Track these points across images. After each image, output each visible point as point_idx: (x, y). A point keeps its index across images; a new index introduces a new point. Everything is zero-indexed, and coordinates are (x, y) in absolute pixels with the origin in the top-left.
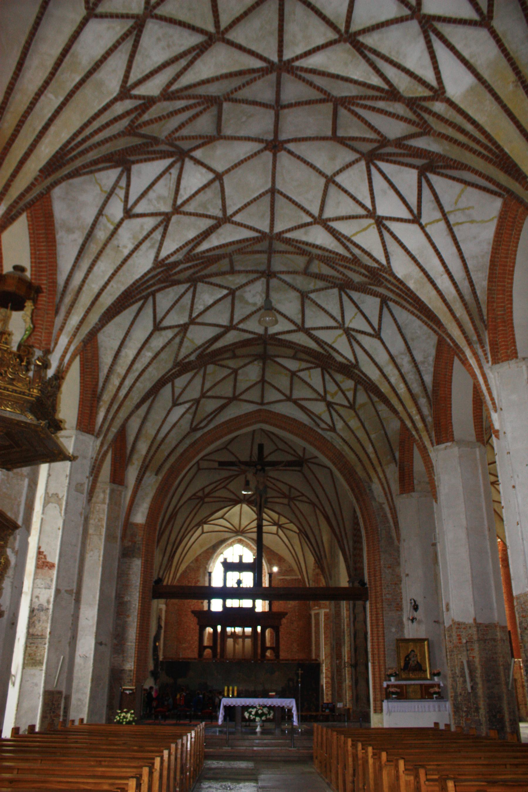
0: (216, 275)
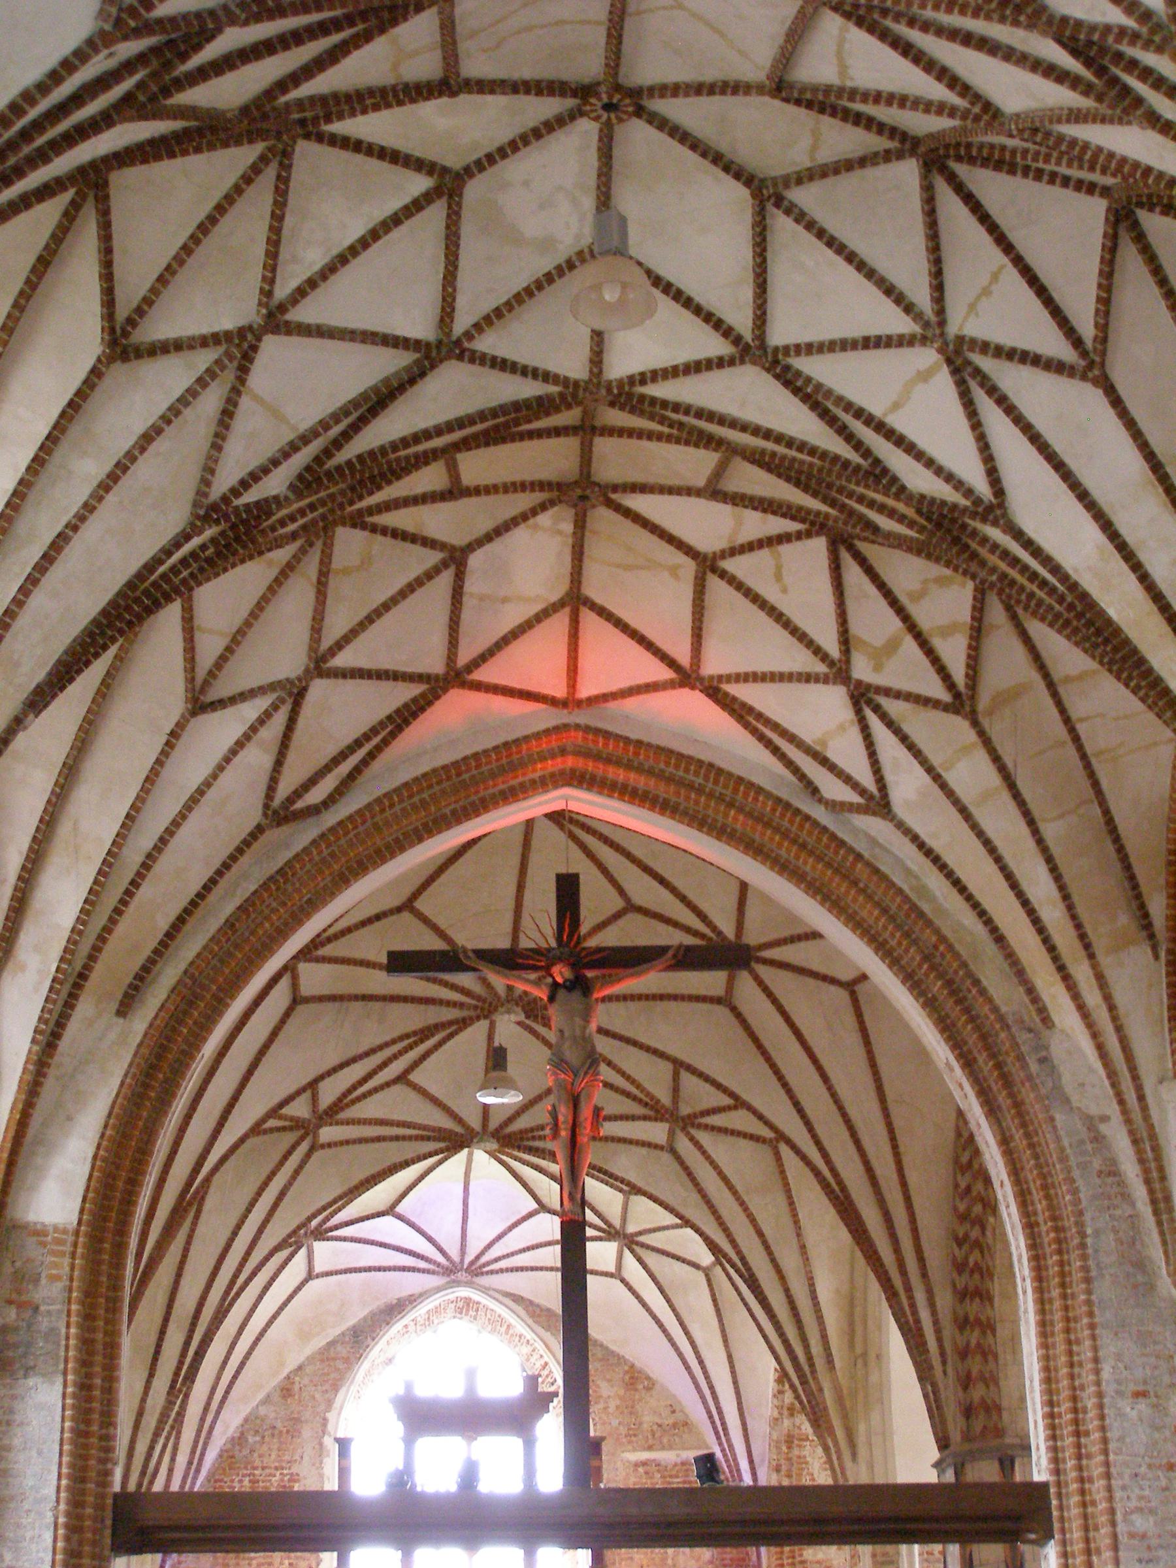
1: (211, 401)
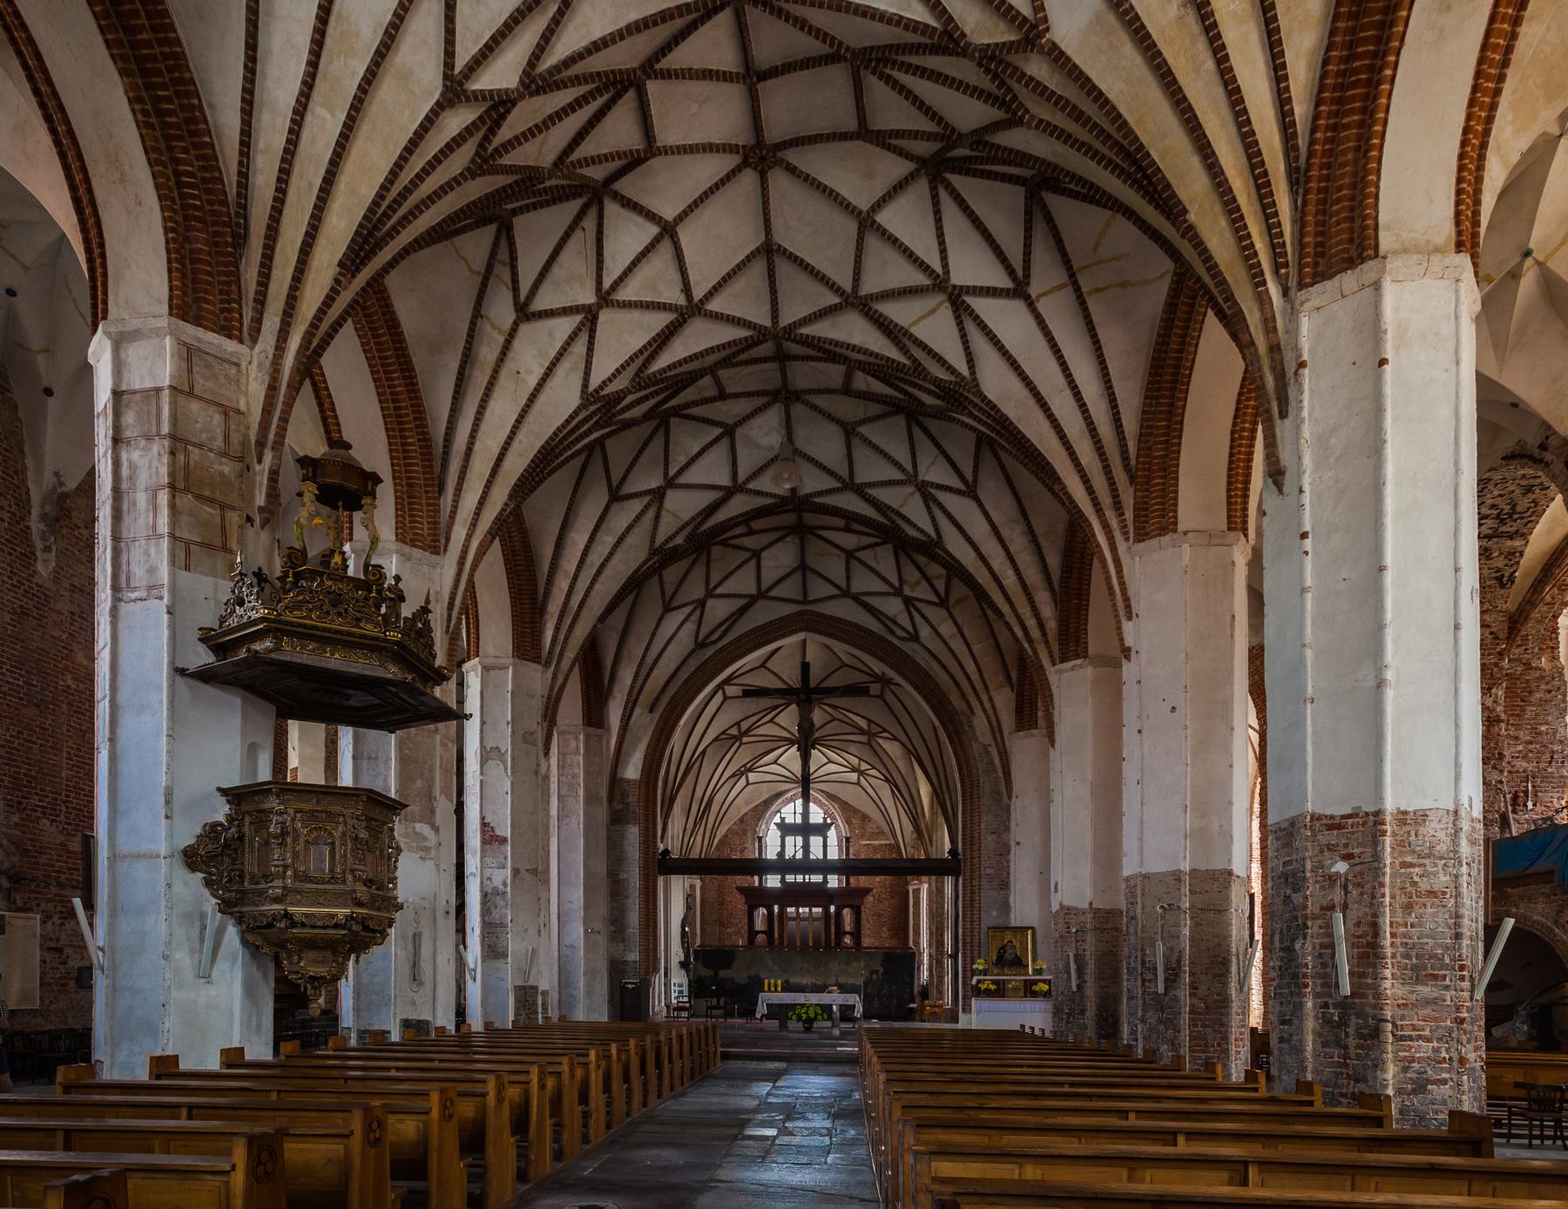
0: (696, 403)
1: (651, 514)
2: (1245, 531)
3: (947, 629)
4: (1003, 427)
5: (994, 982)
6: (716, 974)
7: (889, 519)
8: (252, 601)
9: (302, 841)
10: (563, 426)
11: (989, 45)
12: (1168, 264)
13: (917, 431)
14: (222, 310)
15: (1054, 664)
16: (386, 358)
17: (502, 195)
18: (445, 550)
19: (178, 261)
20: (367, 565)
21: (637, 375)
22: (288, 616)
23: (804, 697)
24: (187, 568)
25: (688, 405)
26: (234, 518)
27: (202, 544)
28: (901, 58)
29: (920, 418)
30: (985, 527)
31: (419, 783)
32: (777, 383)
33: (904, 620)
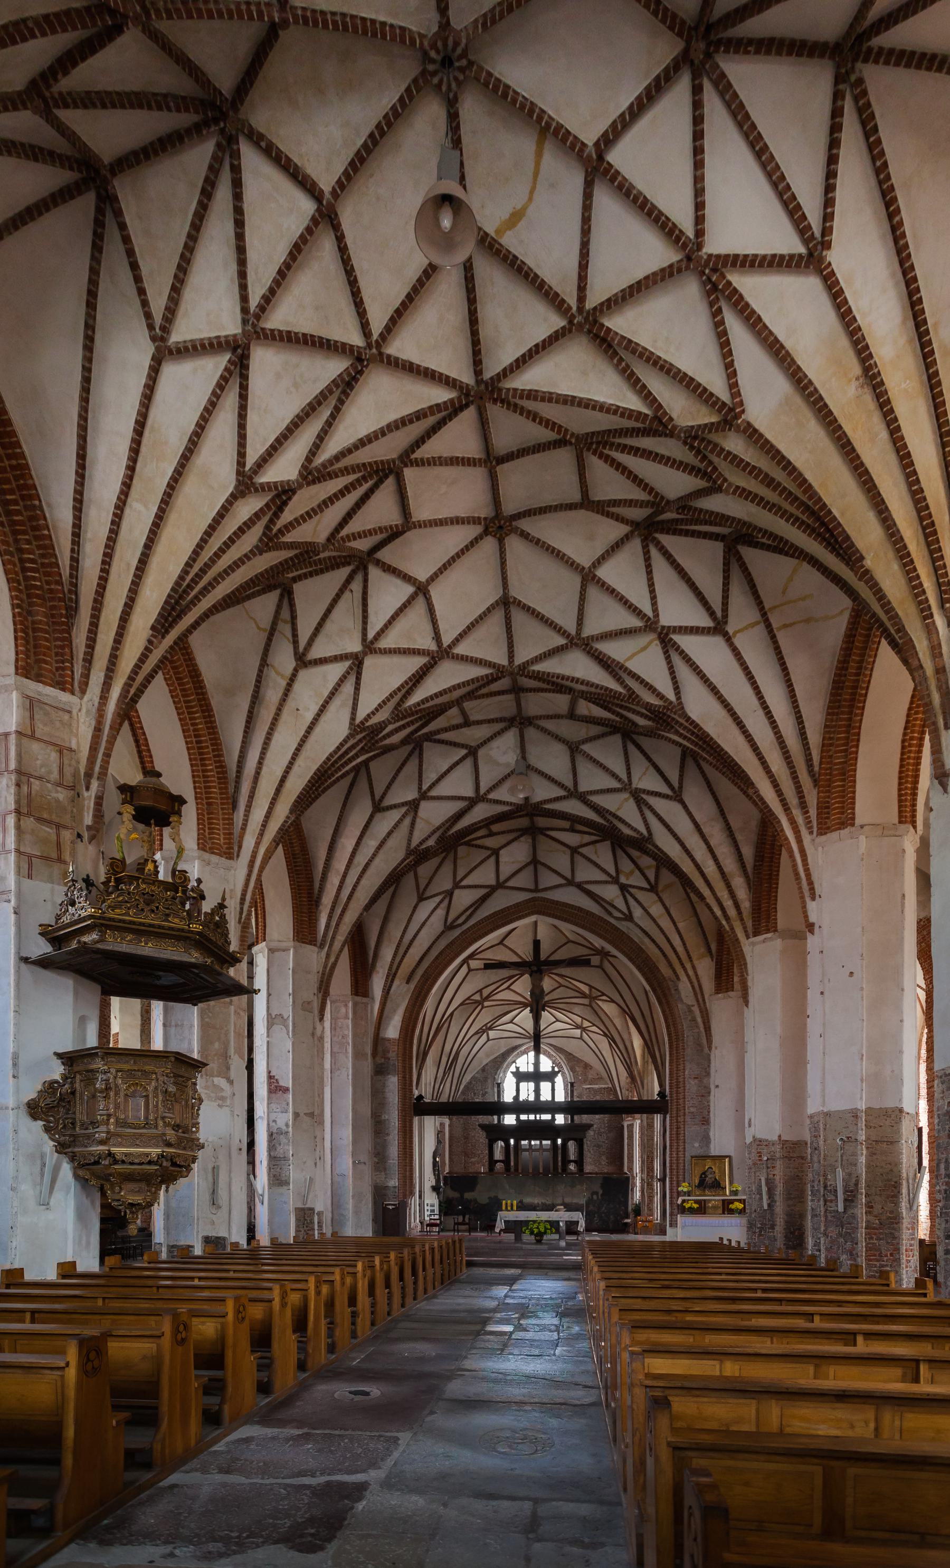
0: (446, 730)
1: (407, 821)
2: (914, 824)
3: (656, 910)
4: (705, 742)
5: (696, 1202)
6: (462, 1196)
7: (608, 821)
8: (81, 902)
9: (122, 1094)
10: (335, 752)
11: (692, 427)
12: (847, 602)
13: (631, 748)
14: (57, 669)
15: (748, 937)
16: (189, 701)
17: (284, 566)
18: (238, 856)
19: (23, 631)
20: (174, 871)
21: (396, 708)
22: (111, 914)
23: (535, 968)
24: (30, 876)
25: (438, 732)
26: (67, 835)
27: (42, 857)
28: (617, 440)
29: (635, 736)
30: (690, 825)
31: (217, 1045)
32: (511, 711)
33: (620, 903)
